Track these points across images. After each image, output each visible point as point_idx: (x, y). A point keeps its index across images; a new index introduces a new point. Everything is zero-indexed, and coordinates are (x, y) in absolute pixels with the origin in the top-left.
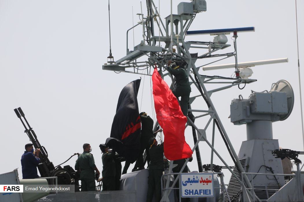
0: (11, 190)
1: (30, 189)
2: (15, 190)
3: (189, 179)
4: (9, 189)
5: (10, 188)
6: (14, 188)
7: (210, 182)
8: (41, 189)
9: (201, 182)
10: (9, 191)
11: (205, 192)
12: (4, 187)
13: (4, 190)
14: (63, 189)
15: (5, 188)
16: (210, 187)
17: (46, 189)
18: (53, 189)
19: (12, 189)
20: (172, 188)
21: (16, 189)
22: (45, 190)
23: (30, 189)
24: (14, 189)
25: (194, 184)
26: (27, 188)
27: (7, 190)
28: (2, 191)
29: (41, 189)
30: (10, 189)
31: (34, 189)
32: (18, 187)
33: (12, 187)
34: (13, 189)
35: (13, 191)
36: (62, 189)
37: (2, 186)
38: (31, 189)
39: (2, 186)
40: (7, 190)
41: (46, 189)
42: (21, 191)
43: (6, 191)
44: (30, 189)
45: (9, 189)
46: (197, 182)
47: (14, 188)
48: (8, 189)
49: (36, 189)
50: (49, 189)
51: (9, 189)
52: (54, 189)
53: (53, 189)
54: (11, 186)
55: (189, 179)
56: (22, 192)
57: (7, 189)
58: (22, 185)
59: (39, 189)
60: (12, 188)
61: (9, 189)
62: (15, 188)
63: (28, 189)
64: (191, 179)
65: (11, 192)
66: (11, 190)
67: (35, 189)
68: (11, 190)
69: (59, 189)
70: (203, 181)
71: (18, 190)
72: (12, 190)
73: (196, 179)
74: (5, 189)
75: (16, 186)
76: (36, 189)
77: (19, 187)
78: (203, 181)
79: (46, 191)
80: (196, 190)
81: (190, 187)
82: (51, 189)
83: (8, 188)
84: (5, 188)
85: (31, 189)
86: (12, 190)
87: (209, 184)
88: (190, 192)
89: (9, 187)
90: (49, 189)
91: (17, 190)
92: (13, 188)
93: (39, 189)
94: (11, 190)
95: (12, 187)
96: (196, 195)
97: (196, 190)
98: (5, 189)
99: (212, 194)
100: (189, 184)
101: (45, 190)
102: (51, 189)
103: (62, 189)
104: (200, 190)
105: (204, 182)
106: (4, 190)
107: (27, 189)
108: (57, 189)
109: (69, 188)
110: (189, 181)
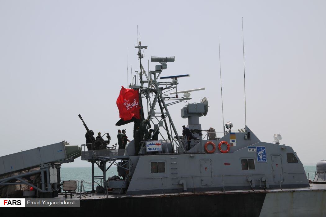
0: (11, 205)
1: (32, 203)
2: (16, 205)
3: (150, 144)
4: (9, 203)
5: (10, 202)
6: (15, 202)
7: (160, 144)
8: (44, 203)
9: (156, 145)
10: (10, 206)
11: (158, 149)
12: (5, 201)
13: (5, 204)
14: (68, 203)
15: (6, 202)
16: (160, 147)
17: (50, 203)
18: (57, 203)
19: (13, 203)
20: (144, 148)
21: (17, 203)
23: (32, 203)
24: (15, 203)
25: (152, 146)
26: (28, 201)
27: (8, 205)
28: (3, 206)
29: (44, 203)
30: (11, 203)
31: (36, 204)
32: (19, 201)
33: (13, 201)
34: (14, 204)
35: (14, 206)
37: (2, 200)
38: (33, 203)
39: (3, 200)
40: (8, 205)
41: (50, 203)
42: (23, 205)
43: (6, 206)
44: (32, 203)
45: (10, 203)
46: (154, 145)
47: (14, 202)
48: (8, 203)
49: (39, 203)
50: (52, 204)
51: (9, 203)
52: (58, 204)
53: (57, 203)
54: (11, 200)
55: (150, 144)
56: (24, 206)
57: (8, 203)
58: (24, 199)
59: (42, 203)
60: (13, 202)
61: (10, 203)
62: (16, 202)
63: (30, 203)
64: (151, 143)
65: (12, 206)
66: (11, 205)
67: (37, 203)
69: (64, 203)
70: (157, 144)
71: (19, 204)
73: (153, 143)
74: (5, 203)
75: (17, 199)
76: (39, 203)
77: (20, 201)
78: (157, 144)
79: (50, 205)
80: (154, 148)
81: (150, 147)
82: (55, 203)
83: (9, 202)
84: (6, 202)
85: (33, 203)
86: (13, 205)
87: (160, 145)
88: (151, 149)
89: (10, 201)
90: (52, 204)
91: (18, 204)
93: (42, 203)
95: (13, 201)
96: (154, 150)
97: (154, 148)
98: (5, 203)
99: (161, 150)
100: (150, 146)
102: (55, 203)
104: (155, 148)
105: (157, 144)
106: (5, 204)
107: (29, 203)
108: (61, 203)
109: (74, 202)
110: (150, 144)
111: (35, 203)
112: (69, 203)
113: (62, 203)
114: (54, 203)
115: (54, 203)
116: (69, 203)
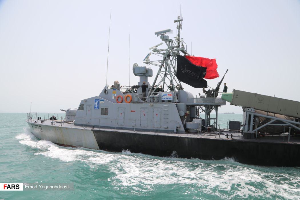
0: (10, 189)
1: (29, 187)
2: (15, 189)
5: (10, 186)
6: (14, 186)
8: (40, 187)
11: (169, 98)
12: (4, 185)
13: (4, 188)
14: (62, 187)
15: (5, 186)
17: (46, 187)
18: (52, 187)
19: (12, 187)
21: (15, 187)
22: (44, 188)
24: (14, 187)
27: (7, 189)
28: (2, 189)
29: (40, 187)
30: (10, 187)
32: (17, 186)
33: (12, 185)
34: (13, 188)
36: (61, 187)
38: (31, 187)
40: (7, 189)
43: (6, 189)
44: (30, 187)
45: (9, 187)
46: (167, 95)
47: (13, 186)
48: (8, 188)
49: (36, 187)
50: (48, 188)
51: (9, 187)
52: (53, 188)
53: (52, 187)
56: (22, 190)
57: (7, 187)
58: (22, 184)
59: (38, 187)
60: (12, 186)
61: (9, 187)
62: (15, 186)
63: (28, 187)
64: (165, 94)
65: (11, 190)
66: (10, 189)
67: (34, 187)
68: (11, 188)
69: (58, 187)
71: (18, 188)
72: (12, 189)
76: (36, 187)
77: (19, 185)
79: (46, 189)
82: (51, 187)
83: (8, 186)
84: (5, 186)
85: (31, 187)
86: (12, 189)
89: (9, 185)
91: (16, 188)
92: (13, 186)
93: (38, 187)
94: (11, 188)
95: (12, 185)
98: (5, 187)
101: (44, 188)
102: (51, 187)
103: (61, 187)
106: (4, 188)
107: (26, 187)
108: (56, 187)
110: (164, 95)
111: (32, 187)
112: (64, 187)
113: (57, 187)
114: (49, 187)
115: (49, 187)
116: (64, 187)
